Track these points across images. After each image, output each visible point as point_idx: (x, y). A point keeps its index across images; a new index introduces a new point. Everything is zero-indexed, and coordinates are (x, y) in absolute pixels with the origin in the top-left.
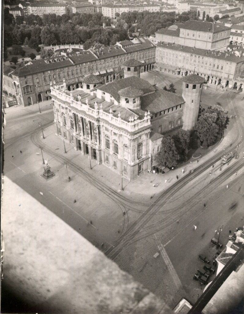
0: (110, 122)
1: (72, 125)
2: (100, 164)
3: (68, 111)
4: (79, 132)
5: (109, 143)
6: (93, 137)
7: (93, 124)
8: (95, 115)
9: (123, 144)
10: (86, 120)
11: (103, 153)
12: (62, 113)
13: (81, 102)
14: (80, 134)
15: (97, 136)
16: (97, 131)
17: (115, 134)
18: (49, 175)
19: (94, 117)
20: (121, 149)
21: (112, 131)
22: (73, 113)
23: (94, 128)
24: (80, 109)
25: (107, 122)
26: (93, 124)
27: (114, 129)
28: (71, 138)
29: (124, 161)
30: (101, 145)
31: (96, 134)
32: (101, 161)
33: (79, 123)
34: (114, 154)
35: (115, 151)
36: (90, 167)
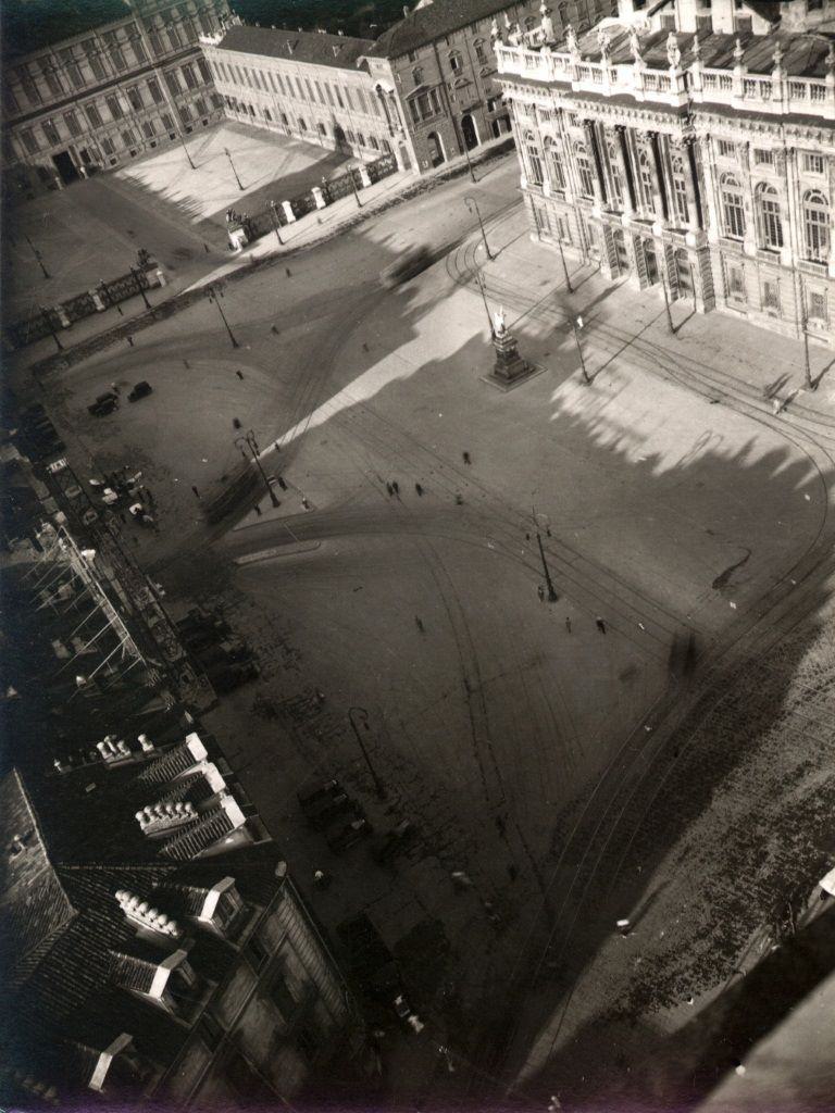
0: (737, 105)
1: (586, 179)
2: (706, 310)
3: (567, 121)
4: (615, 201)
5: (738, 209)
6: (670, 203)
7: (668, 137)
8: (672, 97)
9: (804, 189)
10: (639, 132)
11: (719, 261)
12: (546, 138)
13: (610, 62)
14: (620, 206)
15: (689, 189)
16: (687, 166)
17: (764, 156)
18: (516, 370)
19: (666, 108)
20: (792, 217)
21: (748, 143)
22: (586, 121)
23: (672, 163)
24: (606, 88)
25: (724, 111)
26: (668, 137)
27: (757, 134)
28: (588, 235)
29: (810, 271)
30: (704, 226)
31: (683, 189)
32: (709, 296)
33: (612, 162)
34: (766, 249)
35: (769, 237)
36: (666, 323)
